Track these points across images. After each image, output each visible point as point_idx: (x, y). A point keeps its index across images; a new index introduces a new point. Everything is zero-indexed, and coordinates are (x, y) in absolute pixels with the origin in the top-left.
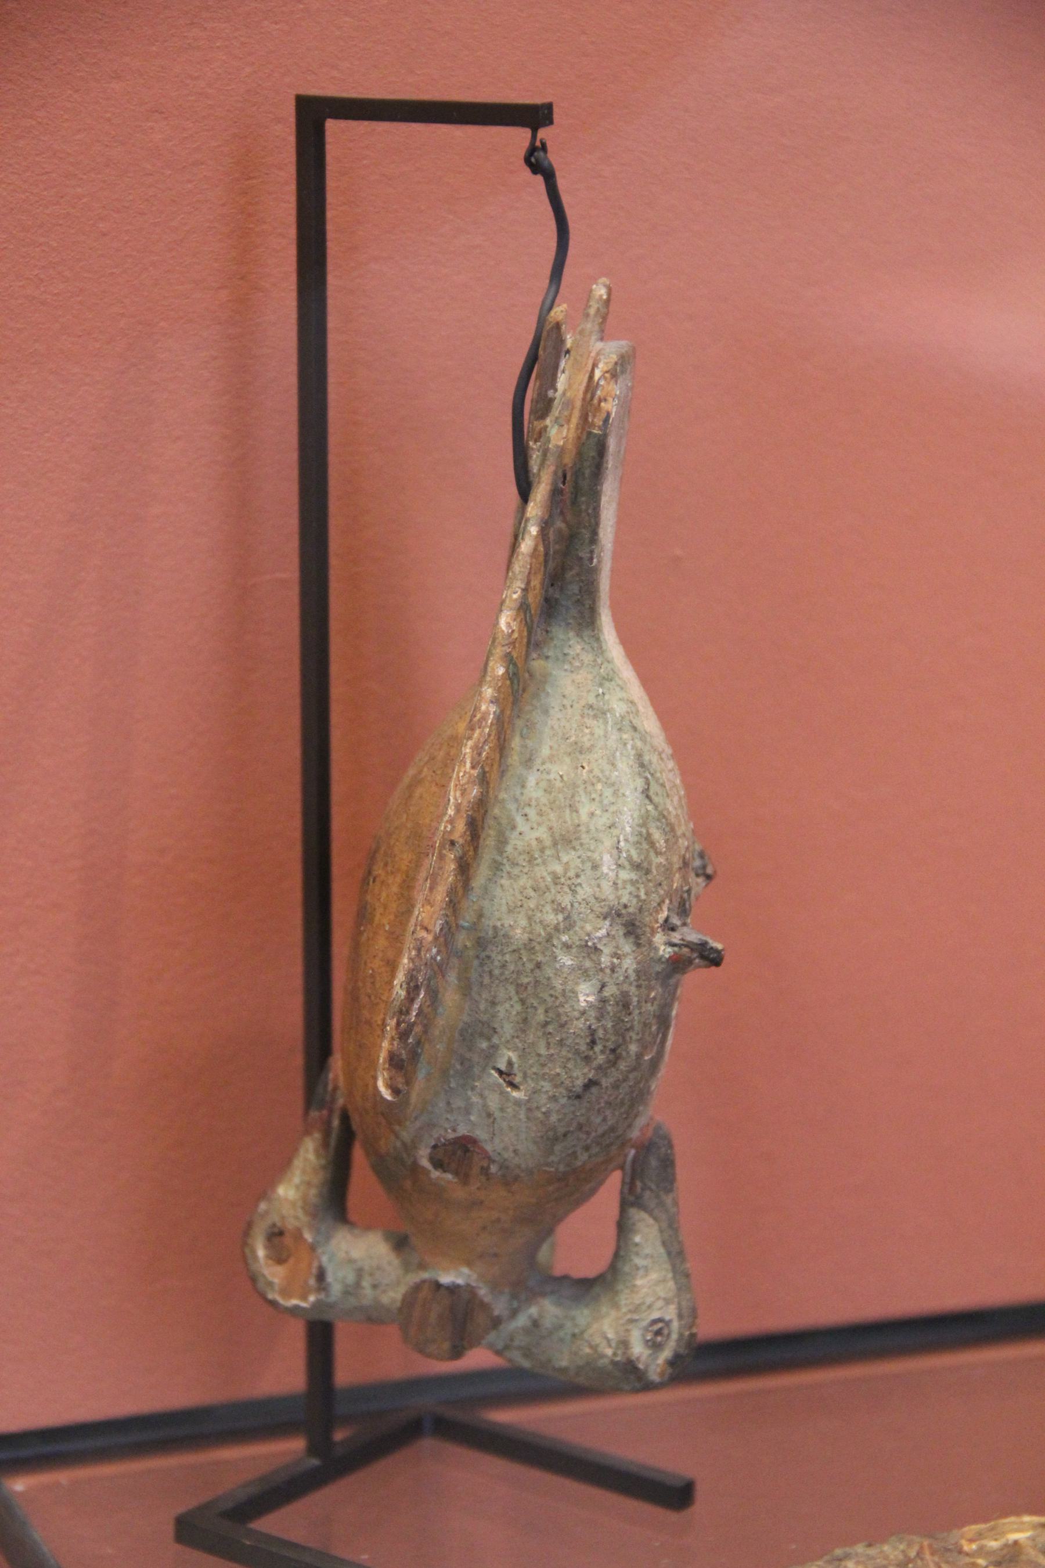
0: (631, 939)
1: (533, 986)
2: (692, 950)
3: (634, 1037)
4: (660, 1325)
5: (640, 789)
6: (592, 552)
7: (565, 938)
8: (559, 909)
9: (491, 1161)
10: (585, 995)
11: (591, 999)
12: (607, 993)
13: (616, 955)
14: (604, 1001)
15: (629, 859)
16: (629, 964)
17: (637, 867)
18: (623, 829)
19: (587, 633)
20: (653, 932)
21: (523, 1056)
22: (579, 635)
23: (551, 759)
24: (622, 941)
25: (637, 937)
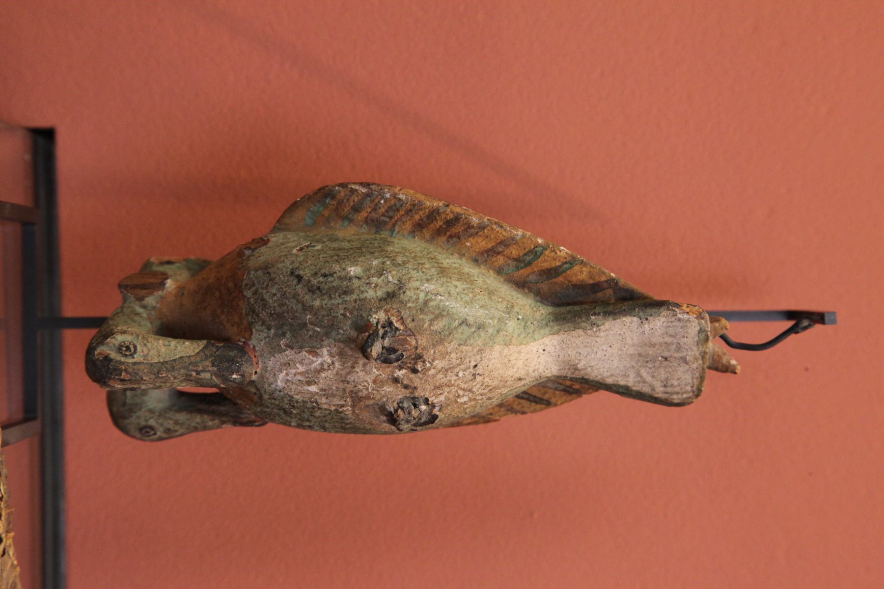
0: (384, 296)
1: (359, 251)
2: (374, 331)
3: (325, 302)
4: (132, 350)
5: (468, 318)
6: (599, 314)
7: (388, 263)
8: (404, 263)
9: (253, 250)
10: (354, 270)
11: (352, 273)
12: (355, 281)
13: (377, 285)
14: (350, 279)
15: (431, 300)
16: (371, 294)
17: (426, 303)
18: (448, 301)
19: (551, 317)
20: (386, 311)
21: (318, 250)
22: (549, 314)
23: (484, 281)
24: (385, 290)
25: (385, 299)
